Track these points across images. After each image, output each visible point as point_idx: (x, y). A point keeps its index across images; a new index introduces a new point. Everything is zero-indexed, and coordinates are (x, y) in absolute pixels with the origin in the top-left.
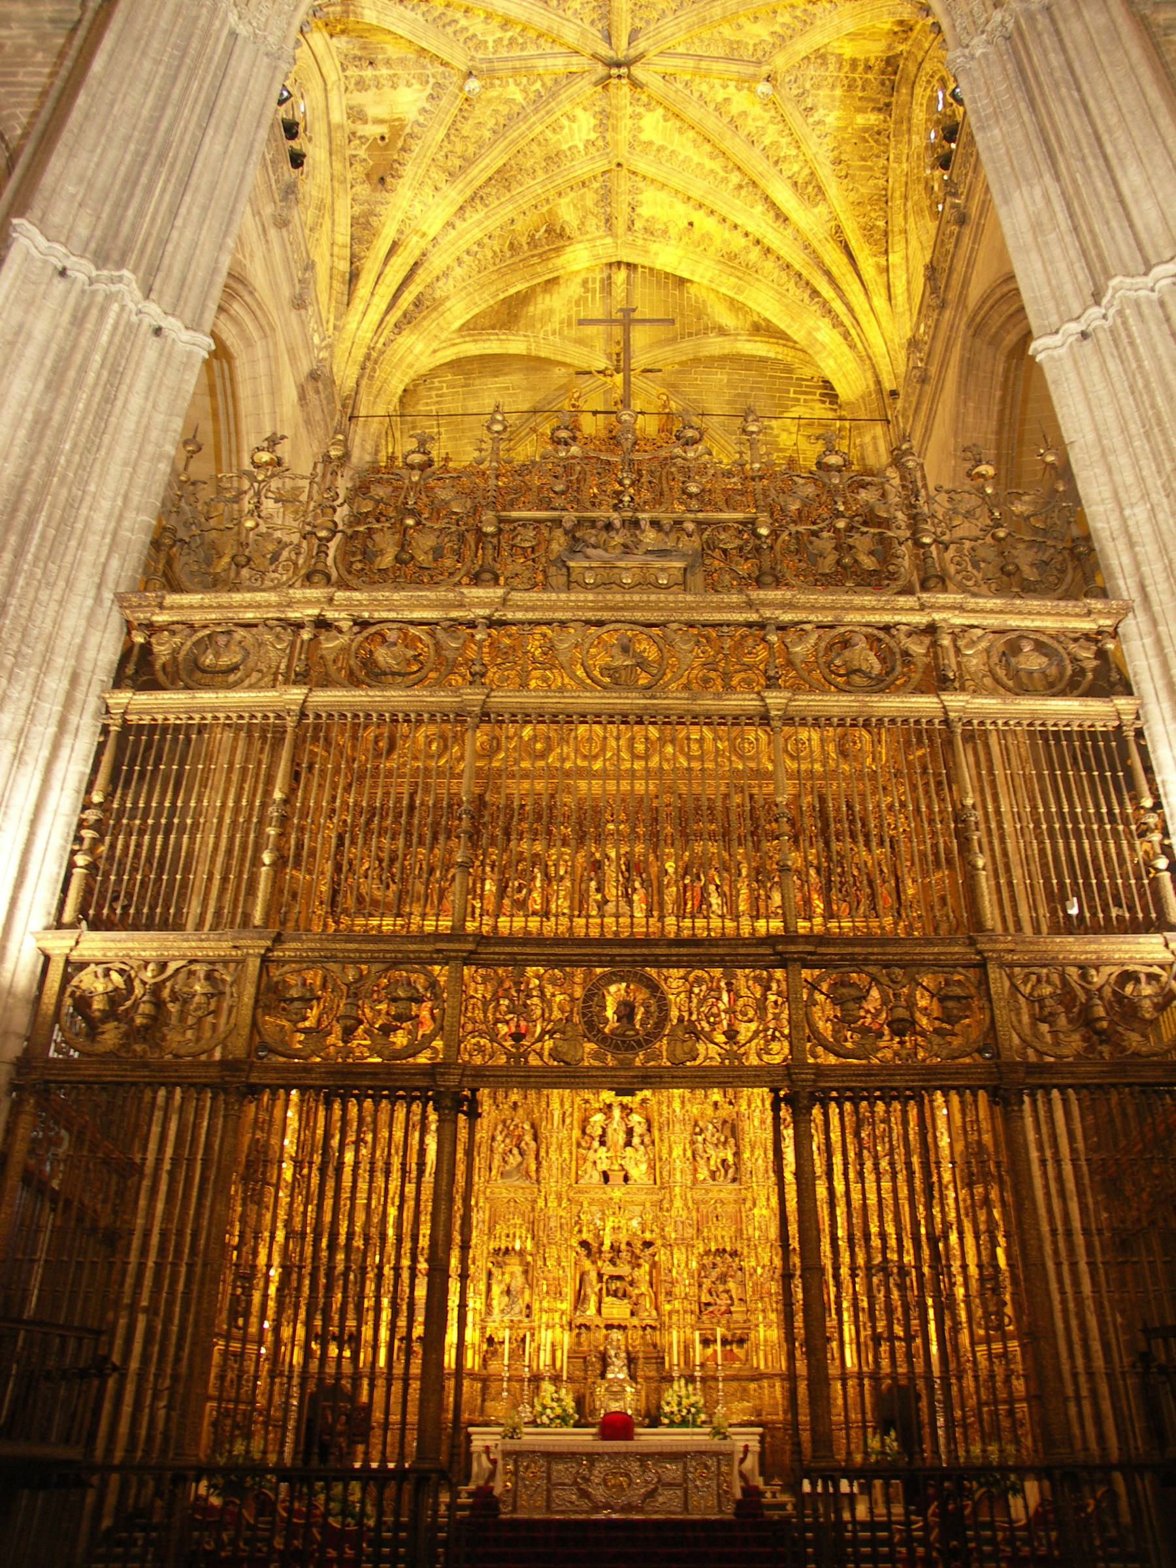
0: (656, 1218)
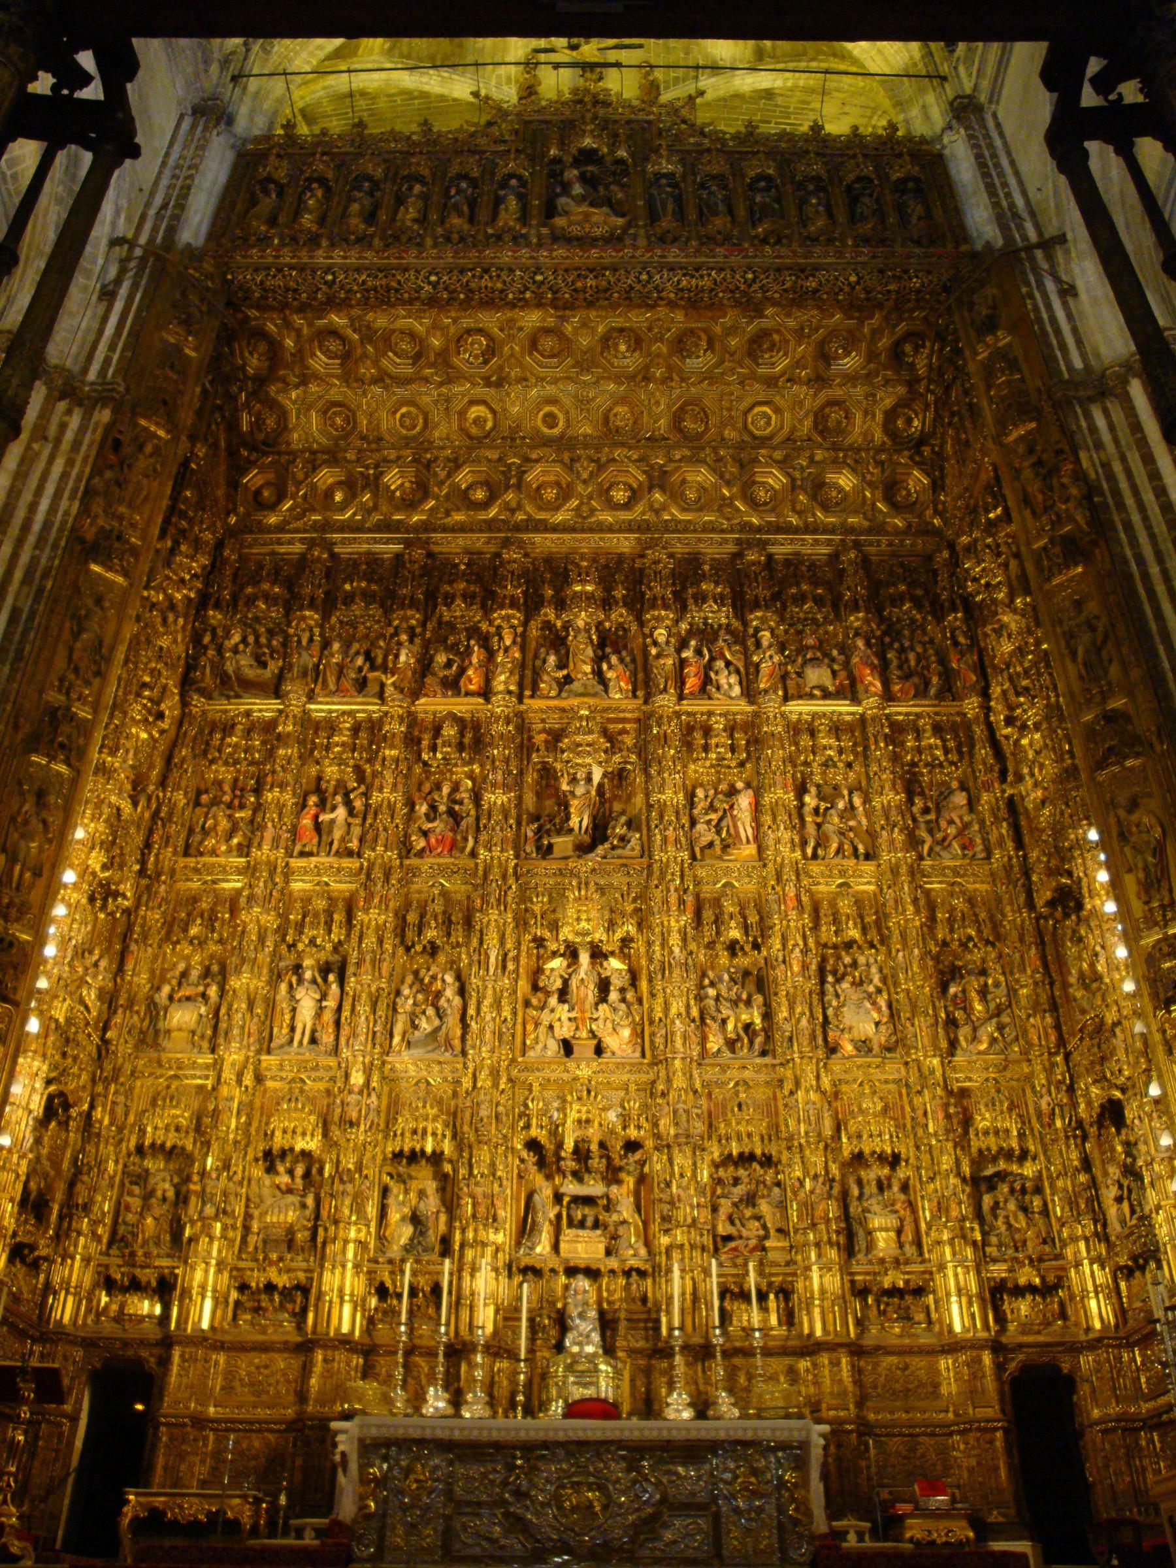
0: (645, 1107)
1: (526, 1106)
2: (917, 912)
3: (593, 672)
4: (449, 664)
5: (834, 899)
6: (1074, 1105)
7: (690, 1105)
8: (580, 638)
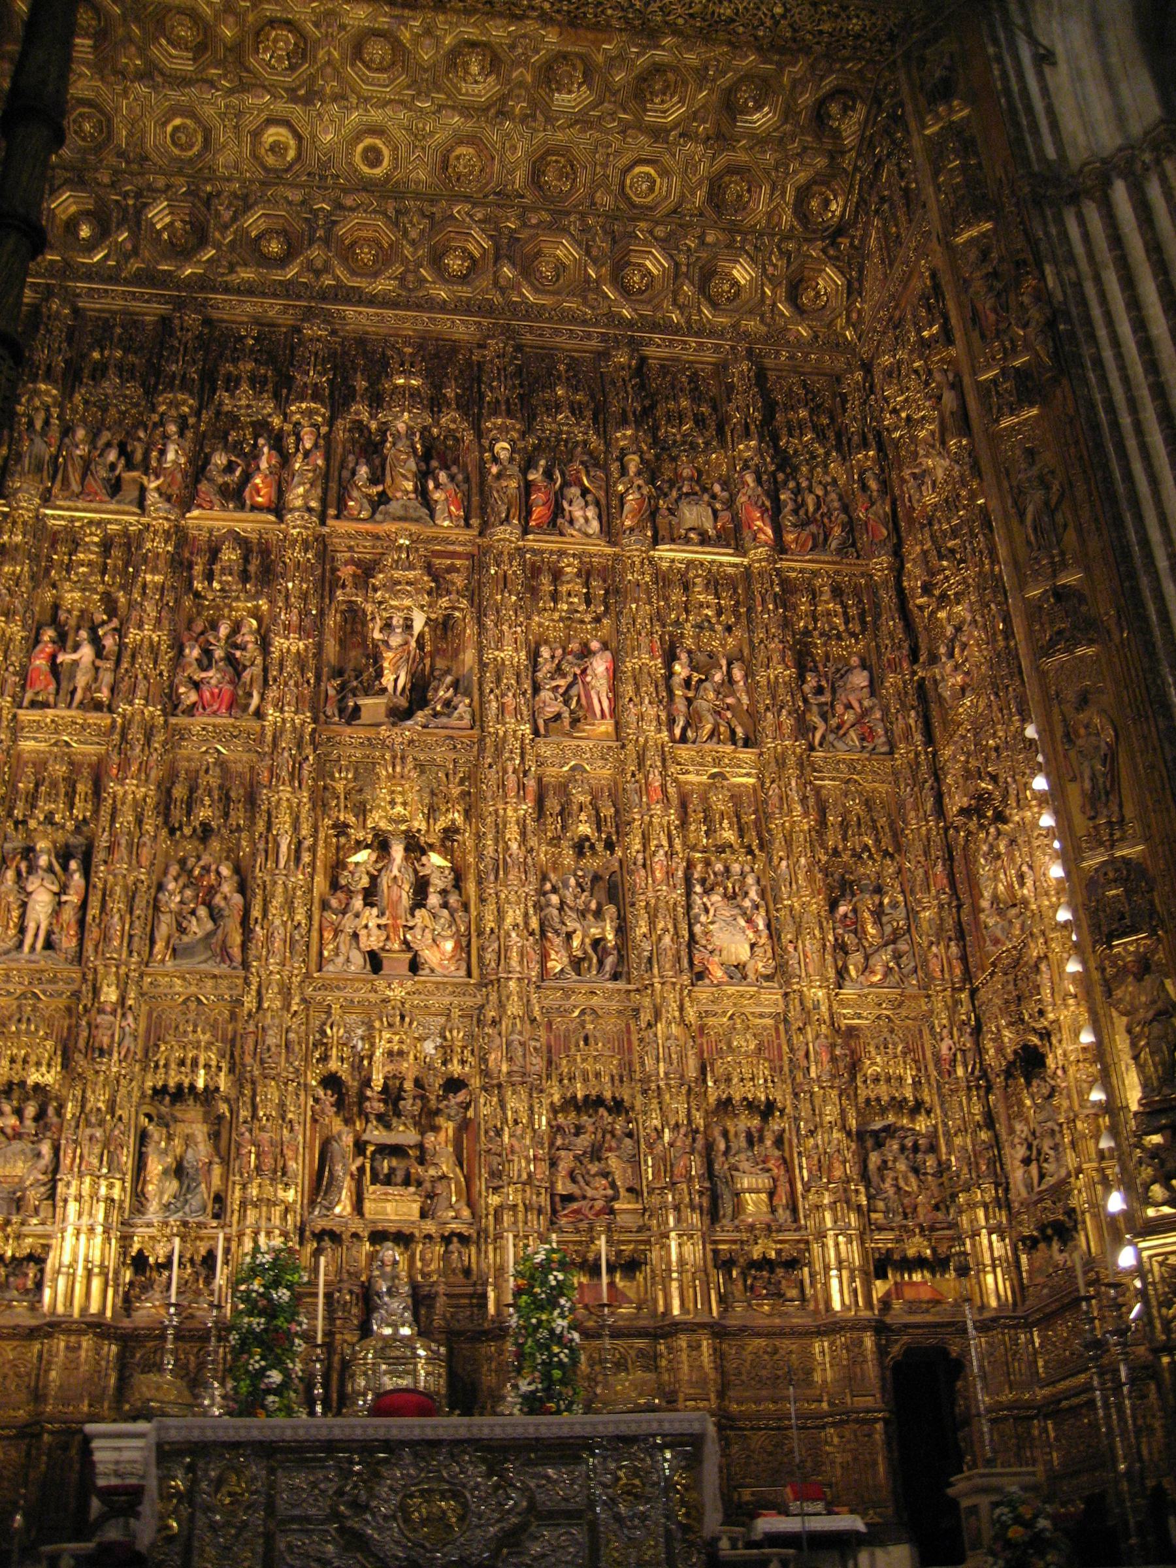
0: (471, 1036)
1: (323, 1033)
2: (806, 814)
3: (416, 490)
4: (230, 468)
5: (706, 792)
6: (980, 1051)
7: (527, 1036)
8: (400, 446)
